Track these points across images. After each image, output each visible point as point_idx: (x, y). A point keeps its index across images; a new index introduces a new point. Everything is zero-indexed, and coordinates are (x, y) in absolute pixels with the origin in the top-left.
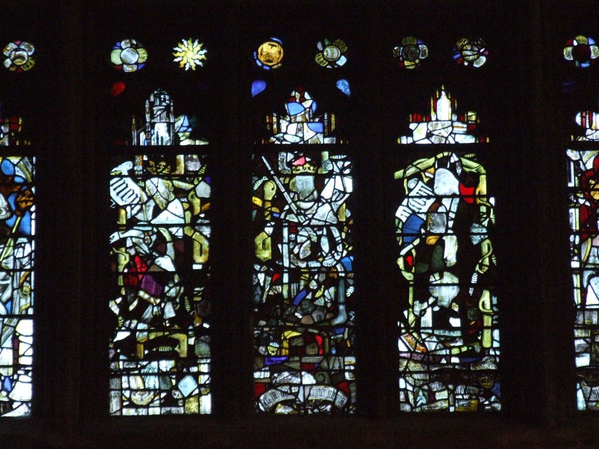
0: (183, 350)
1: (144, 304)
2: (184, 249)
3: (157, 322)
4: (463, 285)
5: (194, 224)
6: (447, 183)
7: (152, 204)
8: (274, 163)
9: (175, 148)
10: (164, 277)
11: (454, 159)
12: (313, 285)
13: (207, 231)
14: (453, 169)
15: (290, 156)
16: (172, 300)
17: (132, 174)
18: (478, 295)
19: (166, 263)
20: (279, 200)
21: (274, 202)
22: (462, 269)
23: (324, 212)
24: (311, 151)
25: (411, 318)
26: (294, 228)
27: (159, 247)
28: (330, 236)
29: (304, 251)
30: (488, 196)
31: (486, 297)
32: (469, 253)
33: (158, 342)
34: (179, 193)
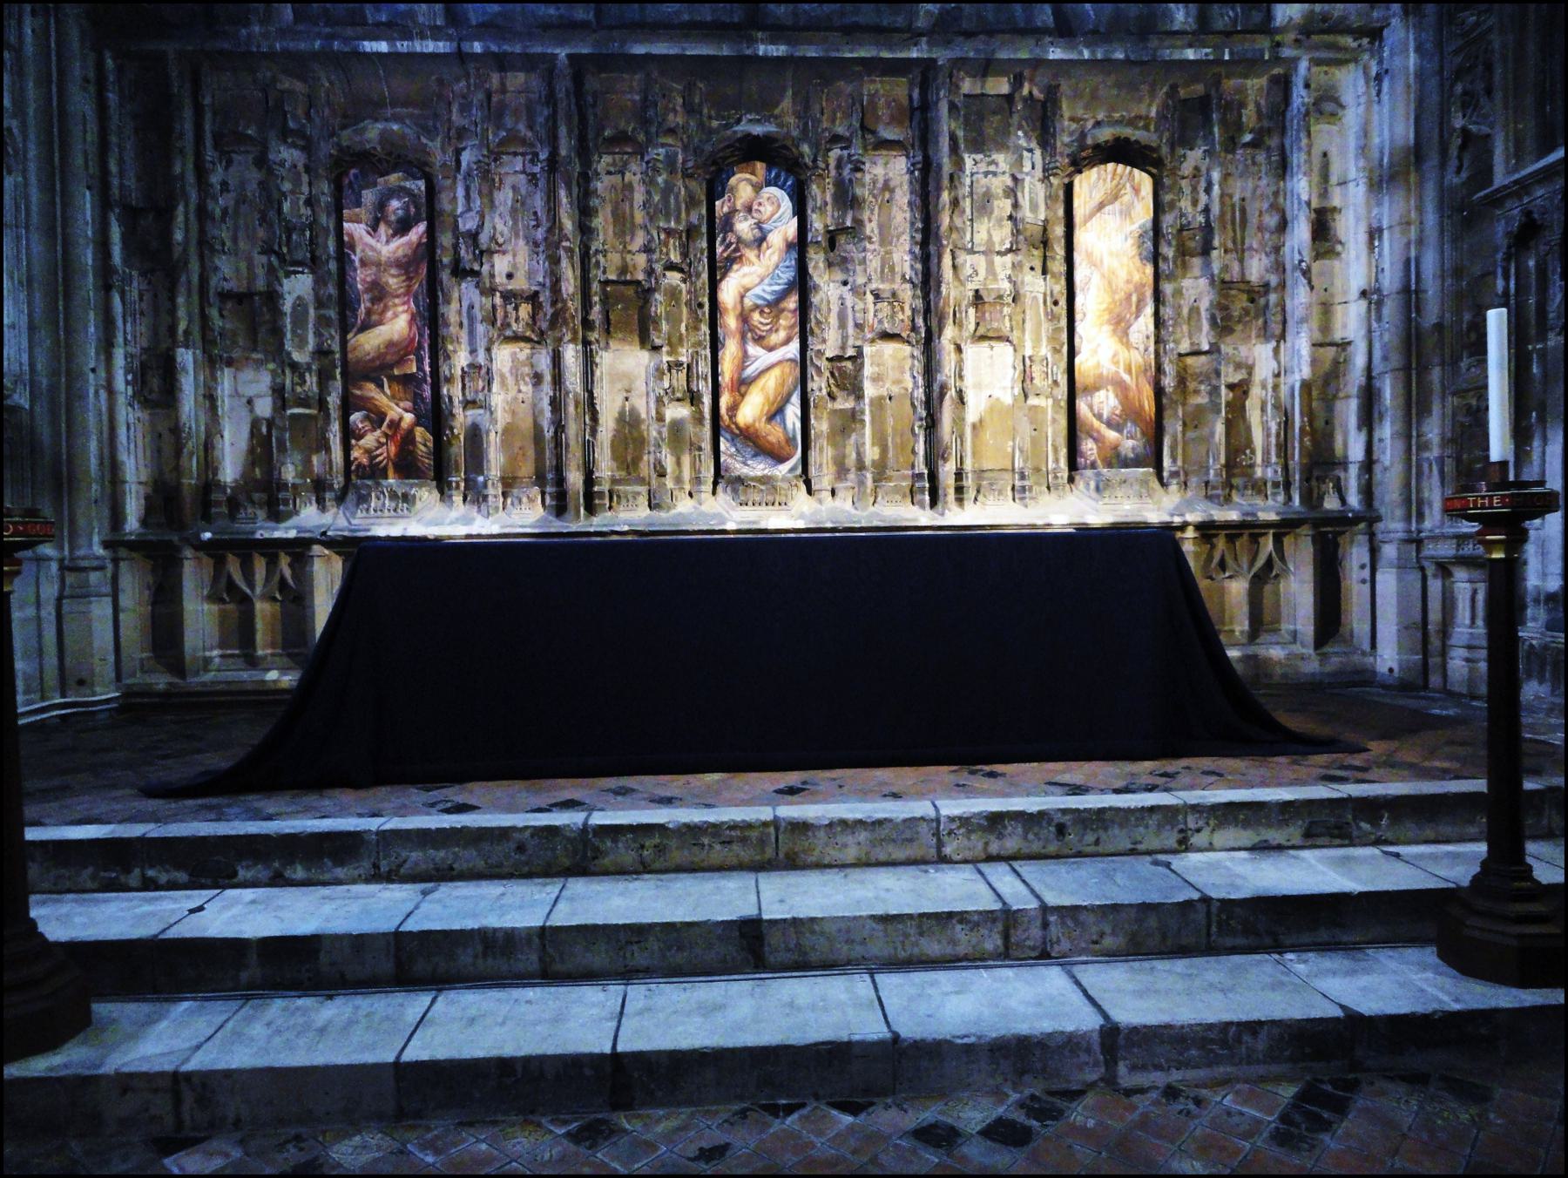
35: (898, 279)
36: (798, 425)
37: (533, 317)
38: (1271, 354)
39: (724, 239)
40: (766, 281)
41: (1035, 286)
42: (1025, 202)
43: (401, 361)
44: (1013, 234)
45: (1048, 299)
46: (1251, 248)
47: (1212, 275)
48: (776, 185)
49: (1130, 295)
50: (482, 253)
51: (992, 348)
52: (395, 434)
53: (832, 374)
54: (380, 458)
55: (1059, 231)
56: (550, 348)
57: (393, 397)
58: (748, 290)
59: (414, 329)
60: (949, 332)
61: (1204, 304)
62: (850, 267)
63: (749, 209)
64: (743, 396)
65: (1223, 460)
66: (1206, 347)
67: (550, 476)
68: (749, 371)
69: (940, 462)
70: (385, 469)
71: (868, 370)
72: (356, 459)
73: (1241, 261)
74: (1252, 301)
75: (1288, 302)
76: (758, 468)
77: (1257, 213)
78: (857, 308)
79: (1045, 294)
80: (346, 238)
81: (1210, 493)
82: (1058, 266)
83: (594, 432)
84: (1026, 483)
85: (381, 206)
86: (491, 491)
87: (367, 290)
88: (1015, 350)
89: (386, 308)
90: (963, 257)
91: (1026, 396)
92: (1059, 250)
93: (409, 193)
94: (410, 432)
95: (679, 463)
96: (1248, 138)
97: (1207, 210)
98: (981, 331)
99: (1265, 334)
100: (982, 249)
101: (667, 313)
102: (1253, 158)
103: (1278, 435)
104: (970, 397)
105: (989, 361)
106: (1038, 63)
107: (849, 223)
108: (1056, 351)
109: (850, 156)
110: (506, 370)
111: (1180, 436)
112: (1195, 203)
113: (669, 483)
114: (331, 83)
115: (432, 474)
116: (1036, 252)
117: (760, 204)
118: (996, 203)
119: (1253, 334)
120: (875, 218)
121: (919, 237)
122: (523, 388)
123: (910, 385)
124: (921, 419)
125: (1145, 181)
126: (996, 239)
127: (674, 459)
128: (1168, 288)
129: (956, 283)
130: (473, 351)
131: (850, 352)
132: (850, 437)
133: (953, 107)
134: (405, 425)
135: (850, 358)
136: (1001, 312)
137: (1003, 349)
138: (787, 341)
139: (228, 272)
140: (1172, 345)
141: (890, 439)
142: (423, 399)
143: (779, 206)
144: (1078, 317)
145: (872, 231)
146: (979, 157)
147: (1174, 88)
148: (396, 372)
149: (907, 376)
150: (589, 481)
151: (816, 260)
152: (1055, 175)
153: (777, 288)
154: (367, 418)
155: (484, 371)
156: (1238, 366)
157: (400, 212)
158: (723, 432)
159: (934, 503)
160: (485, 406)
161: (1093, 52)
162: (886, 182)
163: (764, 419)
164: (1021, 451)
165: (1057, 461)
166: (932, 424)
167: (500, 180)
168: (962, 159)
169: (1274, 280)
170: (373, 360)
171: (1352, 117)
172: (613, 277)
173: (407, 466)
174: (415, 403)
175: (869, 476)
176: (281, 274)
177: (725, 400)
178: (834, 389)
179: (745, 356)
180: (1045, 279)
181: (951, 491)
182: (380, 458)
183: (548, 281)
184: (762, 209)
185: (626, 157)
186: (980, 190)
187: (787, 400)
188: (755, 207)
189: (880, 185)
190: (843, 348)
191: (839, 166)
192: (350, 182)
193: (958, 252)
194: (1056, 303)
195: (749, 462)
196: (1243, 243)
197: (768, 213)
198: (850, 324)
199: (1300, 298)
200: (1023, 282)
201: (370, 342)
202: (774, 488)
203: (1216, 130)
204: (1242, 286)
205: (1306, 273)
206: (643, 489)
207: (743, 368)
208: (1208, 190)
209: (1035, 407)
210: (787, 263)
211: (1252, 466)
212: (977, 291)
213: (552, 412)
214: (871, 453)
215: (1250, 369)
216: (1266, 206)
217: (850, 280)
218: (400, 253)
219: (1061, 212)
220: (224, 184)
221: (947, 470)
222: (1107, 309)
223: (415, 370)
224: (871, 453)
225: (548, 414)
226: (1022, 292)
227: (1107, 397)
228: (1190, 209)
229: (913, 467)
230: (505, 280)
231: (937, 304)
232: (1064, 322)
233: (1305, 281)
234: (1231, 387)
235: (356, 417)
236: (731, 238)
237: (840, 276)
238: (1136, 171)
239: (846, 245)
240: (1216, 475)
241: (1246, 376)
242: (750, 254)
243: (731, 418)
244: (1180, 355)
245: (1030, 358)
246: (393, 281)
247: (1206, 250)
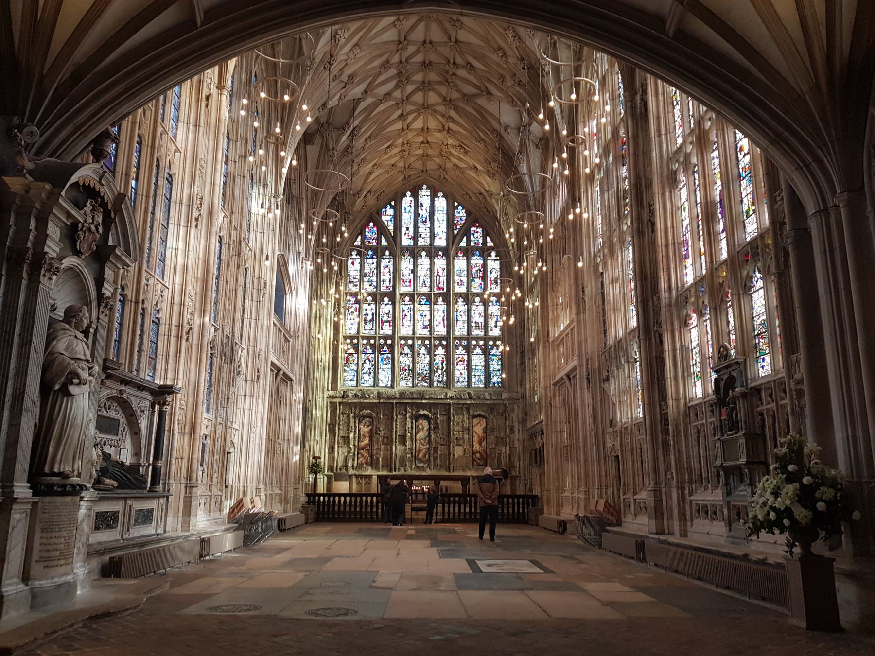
2: (409, 366)
19: (407, 368)
22: (442, 369)
24: (424, 354)
32: (443, 368)
41: (466, 436)
106: (466, 404)
137: (461, 447)
139: (342, 433)
171: (516, 412)
173: (366, 463)
179: (420, 447)
201: (362, 444)
214: (439, 463)
221: (451, 466)
246: (367, 435)
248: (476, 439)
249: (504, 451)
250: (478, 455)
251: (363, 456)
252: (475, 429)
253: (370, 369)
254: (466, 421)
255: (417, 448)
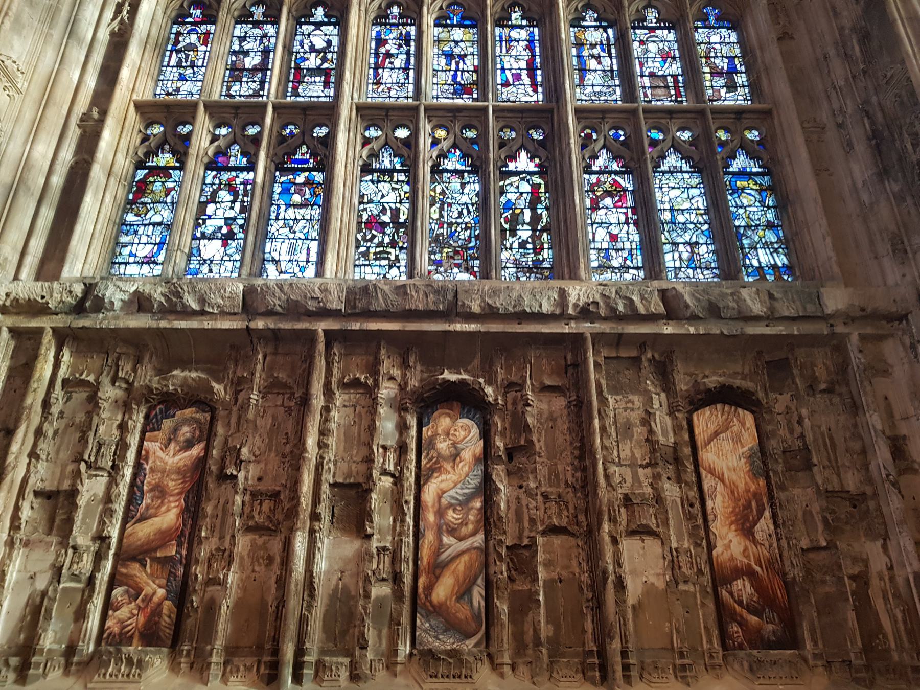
0: (393, 257)
1: (374, 237)
2: (396, 212)
3: (380, 244)
4: (534, 230)
5: (401, 203)
6: (525, 187)
7: (380, 194)
8: (441, 178)
9: (394, 170)
10: (384, 225)
11: (528, 177)
12: (459, 229)
13: (407, 205)
14: (528, 181)
15: (449, 175)
16: (389, 235)
17: (372, 181)
18: (540, 236)
19: (386, 218)
20: (443, 193)
21: (440, 194)
23: (465, 199)
24: (460, 173)
25: (508, 246)
26: (450, 205)
27: (384, 211)
28: (468, 208)
29: (456, 215)
30: (545, 193)
31: (545, 235)
32: (536, 218)
33: (380, 252)
34: (393, 189)
35: (563, 485)
36: (483, 604)
37: (273, 511)
38: (881, 550)
39: (428, 454)
40: (459, 486)
41: (671, 491)
42: (658, 429)
43: (163, 545)
44: (650, 452)
45: (685, 502)
46: (844, 465)
47: (818, 487)
48: (467, 417)
49: (750, 503)
50: (241, 461)
51: (643, 541)
52: (147, 606)
53: (511, 559)
54: (130, 627)
55: (687, 451)
56: (283, 536)
57: (152, 576)
58: (444, 492)
59: (181, 520)
60: (606, 526)
61: (816, 508)
62: (524, 475)
63: (448, 434)
64: (437, 578)
65: (860, 644)
66: (824, 544)
67: (267, 646)
68: (444, 556)
69: (608, 640)
70: (132, 637)
71: (540, 557)
72: (109, 628)
73: (839, 475)
74: (855, 507)
75: (885, 509)
76: (448, 643)
77: (843, 439)
78: (530, 506)
79: (682, 499)
80: (143, 453)
81: (854, 675)
82: (691, 478)
83: (310, 607)
84: (686, 661)
85: (175, 430)
86: (214, 659)
87: (151, 490)
88: (663, 543)
89: (162, 504)
90: (613, 469)
91: (677, 584)
92: (690, 467)
93: (197, 421)
94: (160, 604)
95: (379, 637)
96: (823, 386)
97: (802, 436)
98: (634, 527)
99: (872, 535)
100: (627, 463)
101: (380, 508)
102: (830, 400)
103: (905, 622)
104: (629, 582)
105: (641, 552)
107: (522, 443)
108: (697, 545)
109: (522, 396)
110: (245, 553)
111: (816, 623)
112: (791, 432)
113: (370, 655)
114: (155, 348)
115: (170, 642)
116: (670, 467)
117: (456, 430)
118: (635, 429)
119: (862, 533)
120: (543, 439)
121: (577, 452)
122: (257, 568)
123: (577, 570)
124: (588, 601)
125: (749, 419)
126: (638, 455)
127: (376, 632)
128: (780, 496)
129: (609, 488)
130: (222, 538)
131: (526, 542)
132: (527, 615)
133: (597, 365)
134: (156, 599)
135: (526, 547)
136: (648, 512)
138: (474, 534)
140: (794, 541)
141: (562, 618)
142: (175, 576)
143: (470, 432)
144: (710, 517)
145: (541, 448)
146: (618, 398)
147: (760, 353)
148: (159, 555)
149: (574, 563)
150: (300, 652)
151: (499, 471)
152: (679, 411)
153: (467, 491)
154: (127, 592)
155: (227, 554)
156: (855, 560)
157: (188, 435)
158: (419, 609)
159: (604, 678)
160: (223, 583)
161: (696, 329)
162: (551, 413)
163: (454, 598)
164: (678, 632)
165: (710, 641)
166: (599, 605)
167: (264, 410)
168: (607, 399)
169: (869, 490)
170: (142, 546)
172: (340, 480)
174: (168, 581)
175: (544, 651)
176: (84, 476)
177: (422, 581)
178: (513, 572)
180: (680, 487)
181: (619, 668)
182: (130, 627)
183: (288, 482)
184: (457, 434)
185: (358, 396)
186: (621, 420)
187: (474, 582)
188: (452, 432)
189: (545, 416)
190: (520, 538)
191: (515, 403)
192: (156, 415)
193: (608, 464)
194: (692, 505)
195: (441, 637)
196: (837, 462)
197: (462, 437)
198: (526, 518)
199: (894, 505)
200: (663, 488)
201: (143, 531)
202: (461, 661)
203: (797, 380)
204: (843, 495)
205: (894, 484)
206: (346, 661)
207: (439, 555)
208: (800, 422)
209: (685, 591)
210: (475, 473)
211: (888, 650)
212: (626, 495)
213: (277, 589)
214: (545, 630)
215: (866, 562)
216: (848, 435)
217: (525, 484)
218: (181, 464)
219: (686, 437)
220: (61, 413)
222: (732, 512)
223: (174, 553)
224: (545, 630)
225: (273, 591)
226: (663, 496)
227: (744, 585)
228: (788, 436)
229: (584, 644)
230: (256, 482)
231: (594, 504)
232: (700, 521)
233: (896, 491)
234: (852, 578)
235: (118, 592)
236: (433, 453)
237: (516, 483)
238: (740, 410)
239: (521, 460)
240: (856, 658)
241: (863, 569)
242: (448, 466)
243: (426, 597)
244: (802, 549)
245: (676, 550)
246: (172, 485)
247: (808, 466)
248: (718, 504)
249: (878, 563)
250: (743, 587)
251: (135, 592)
252: (708, 456)
253: (229, 221)
254: (662, 422)
255: (425, 553)
